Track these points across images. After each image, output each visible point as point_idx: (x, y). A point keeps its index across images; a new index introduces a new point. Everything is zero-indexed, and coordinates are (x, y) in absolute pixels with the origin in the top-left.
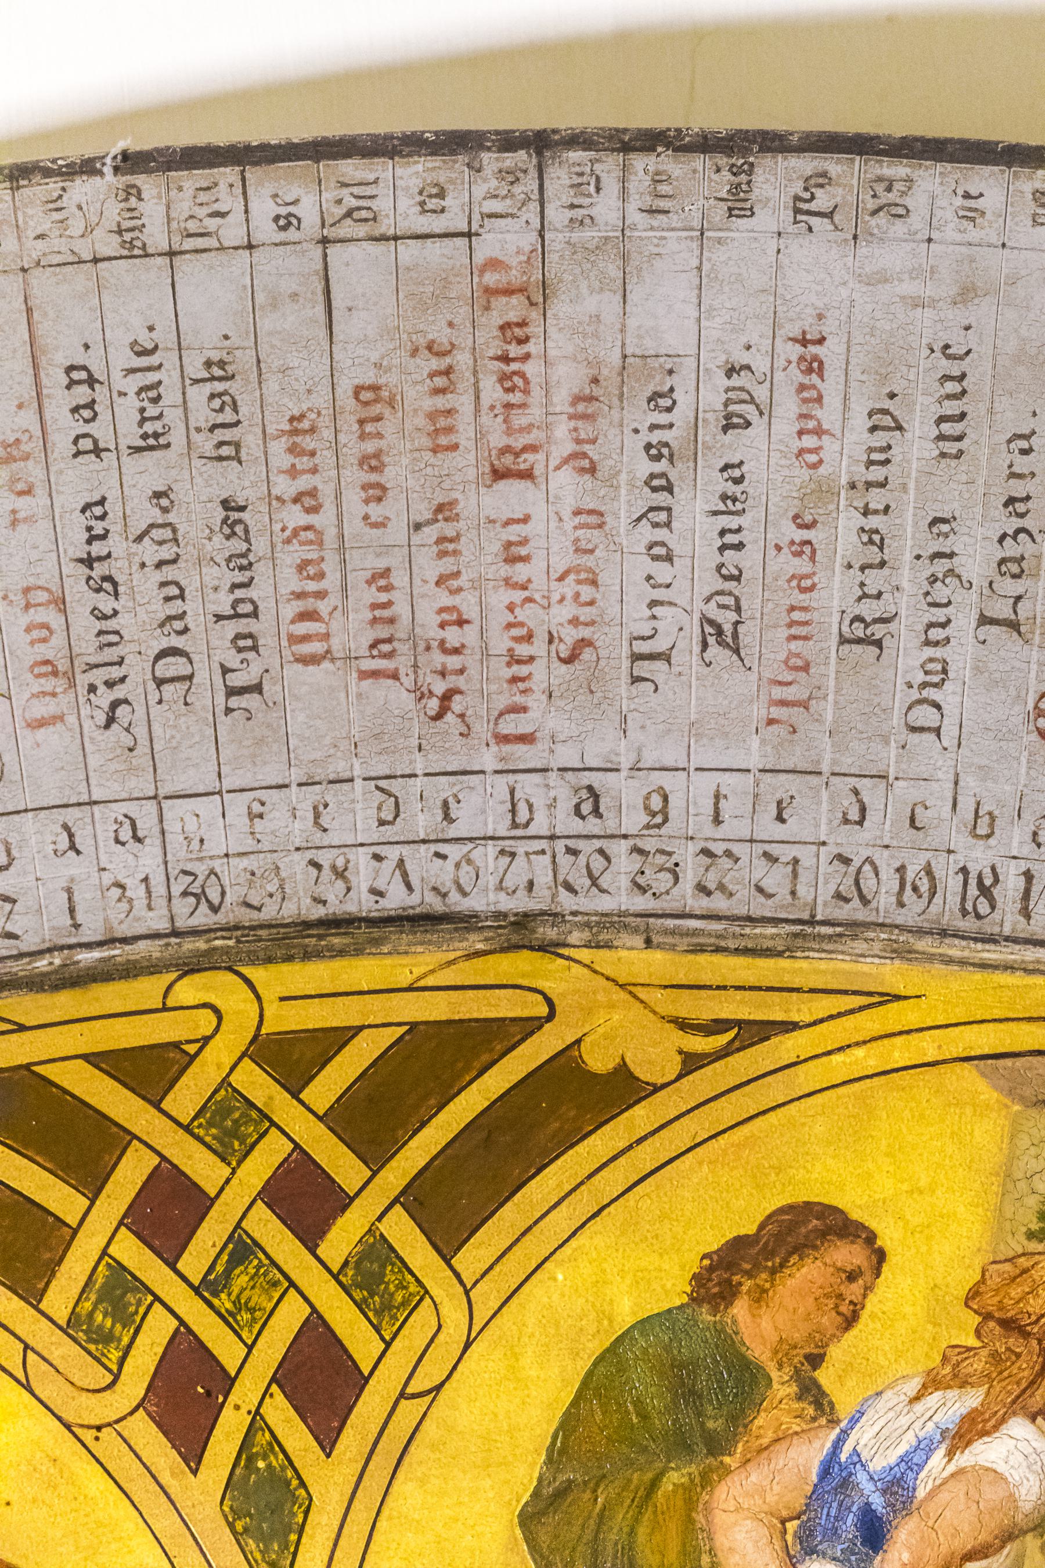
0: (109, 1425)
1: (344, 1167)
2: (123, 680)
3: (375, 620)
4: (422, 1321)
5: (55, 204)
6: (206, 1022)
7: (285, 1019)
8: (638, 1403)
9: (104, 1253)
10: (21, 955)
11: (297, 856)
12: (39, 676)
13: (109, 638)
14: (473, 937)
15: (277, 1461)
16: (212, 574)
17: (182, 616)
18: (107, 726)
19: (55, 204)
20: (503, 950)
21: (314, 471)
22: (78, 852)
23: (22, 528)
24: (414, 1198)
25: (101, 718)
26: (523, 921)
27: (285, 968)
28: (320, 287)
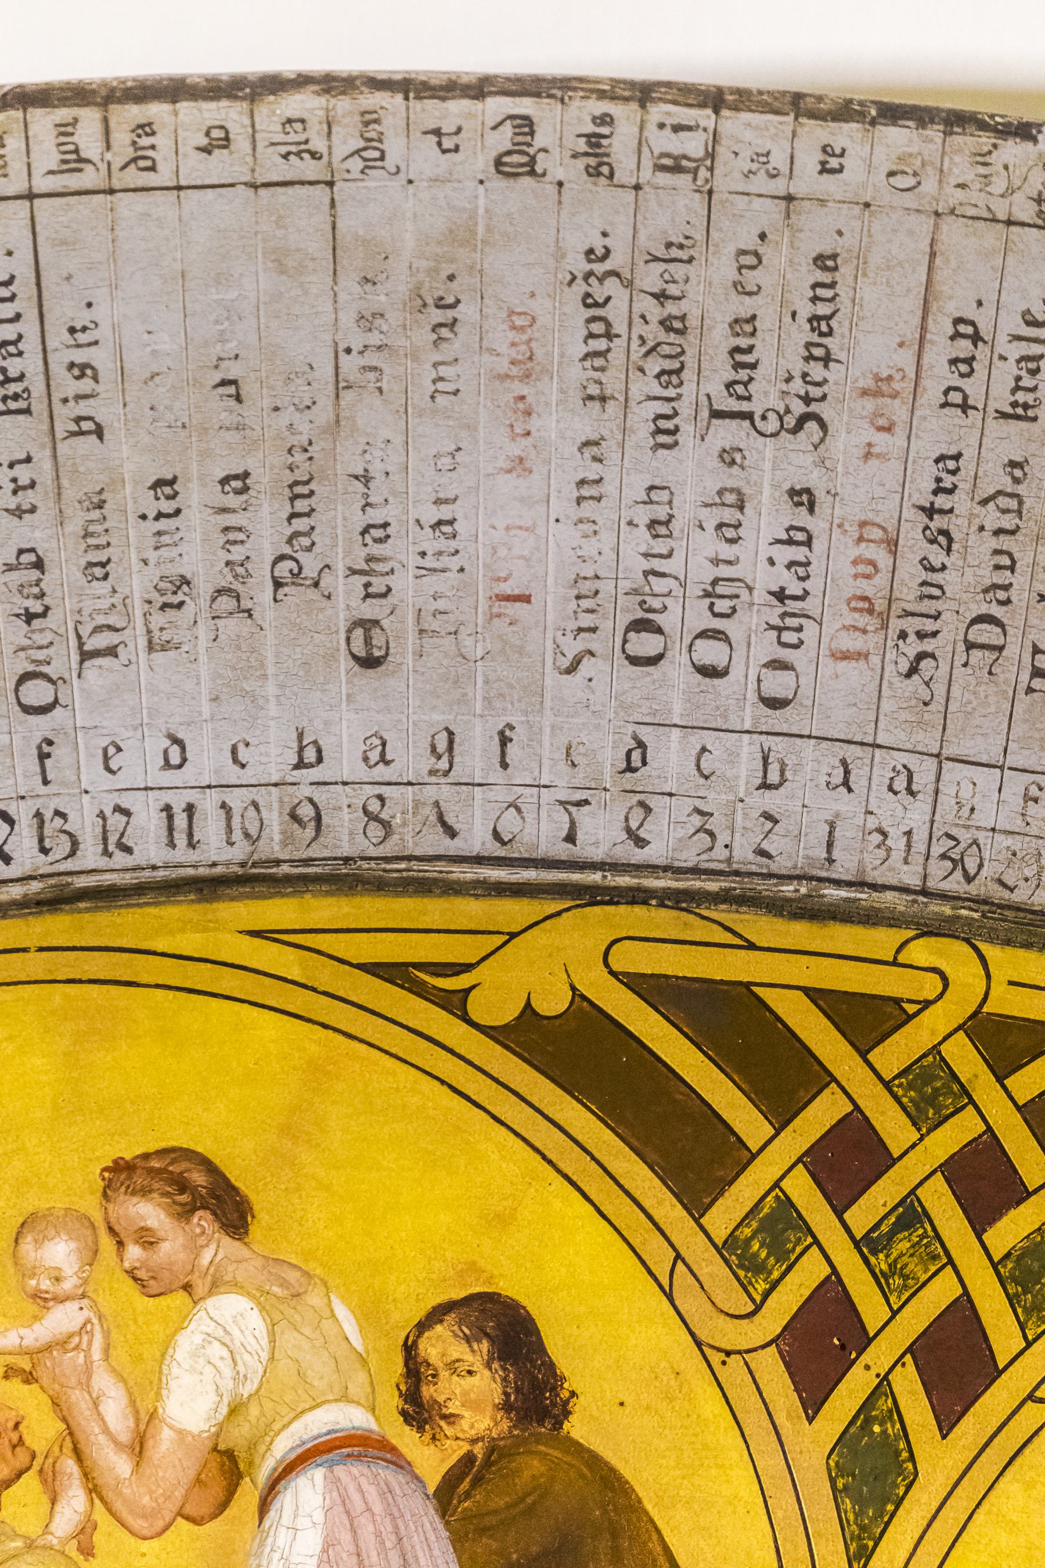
0: (739, 1352)
2: (935, 634)
5: (982, 159)
6: (931, 986)
9: (777, 1185)
10: (771, 875)
12: (855, 610)
15: (893, 1429)
17: (1006, 588)
18: (908, 675)
19: (982, 159)
22: (850, 790)
23: (874, 462)
25: (904, 666)
27: (1021, 953)
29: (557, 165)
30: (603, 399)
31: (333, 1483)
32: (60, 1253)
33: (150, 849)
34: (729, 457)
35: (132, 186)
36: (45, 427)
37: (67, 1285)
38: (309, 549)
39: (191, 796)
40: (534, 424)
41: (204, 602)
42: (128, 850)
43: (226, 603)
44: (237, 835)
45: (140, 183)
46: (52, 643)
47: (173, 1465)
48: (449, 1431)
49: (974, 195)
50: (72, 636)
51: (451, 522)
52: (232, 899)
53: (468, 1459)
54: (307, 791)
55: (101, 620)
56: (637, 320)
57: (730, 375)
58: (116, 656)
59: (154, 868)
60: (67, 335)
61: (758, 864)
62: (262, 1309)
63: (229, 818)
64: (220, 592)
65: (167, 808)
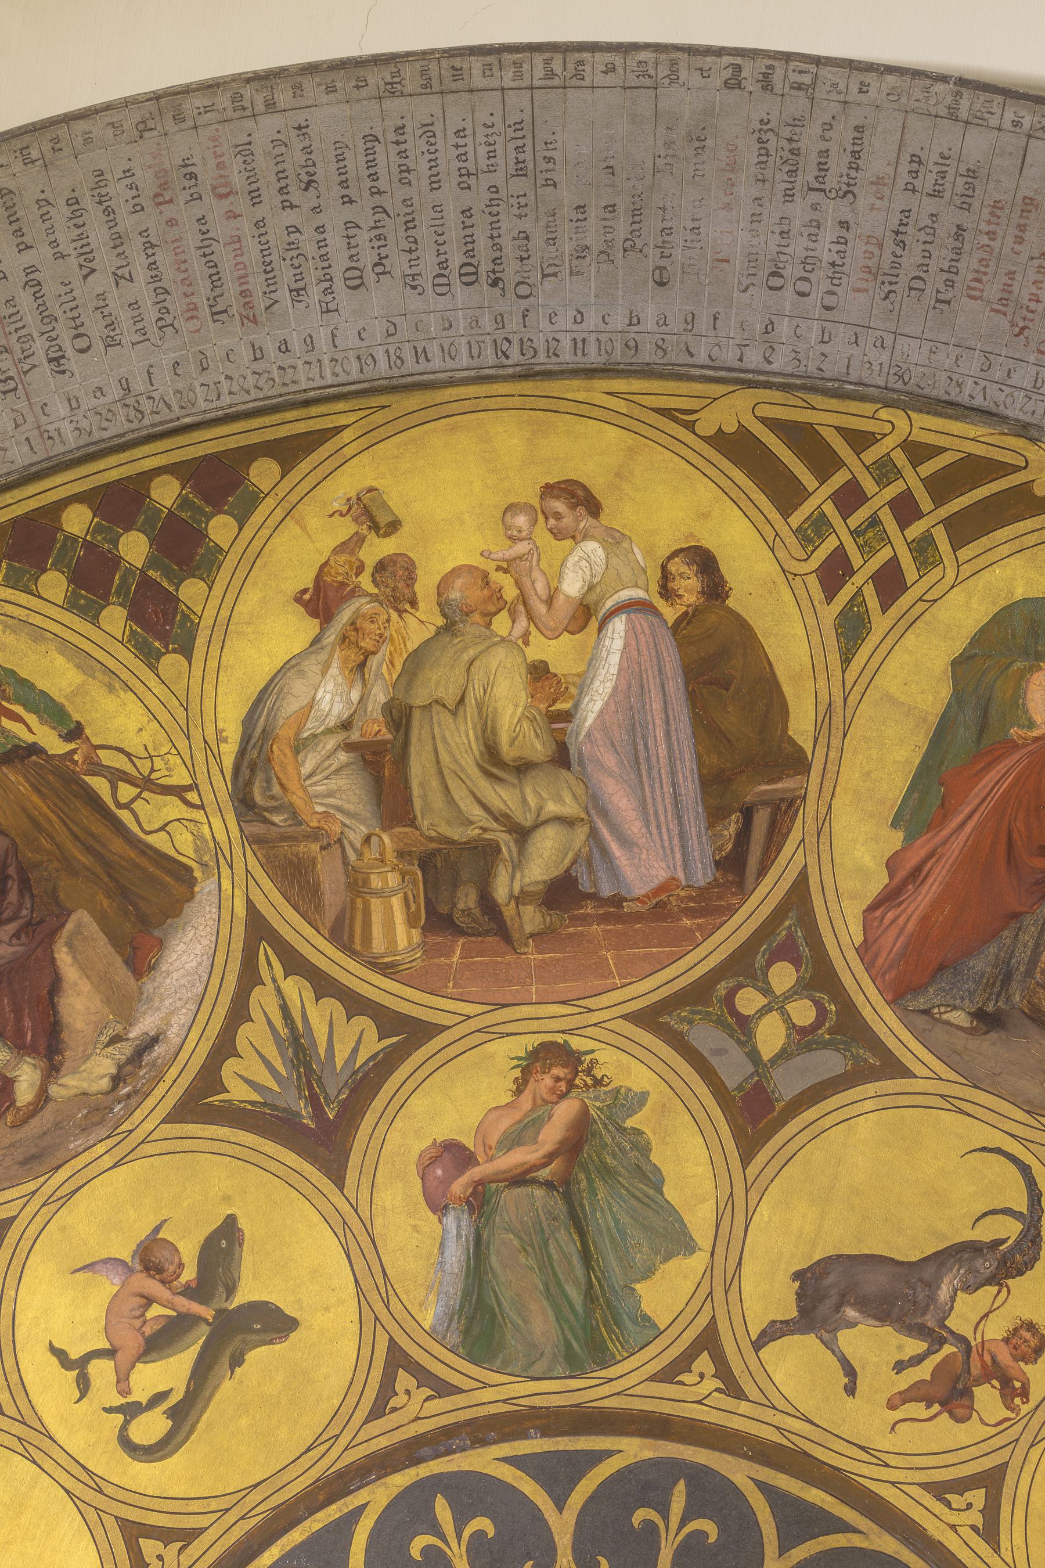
1: (925, 502)
2: (896, 283)
3: (1004, 290)
4: (937, 572)
6: (888, 428)
7: (919, 436)
8: (1013, 631)
9: (819, 507)
10: (823, 379)
11: (944, 373)
13: (896, 265)
14: (1004, 426)
15: (862, 610)
16: (944, 252)
18: (884, 299)
19: (926, 90)
20: (1015, 436)
21: (998, 224)
23: (874, 212)
24: (948, 523)
25: (883, 295)
26: (1026, 426)
27: (925, 416)
28: (1022, 153)
29: (750, 86)
30: (764, 181)
31: (629, 621)
32: (521, 520)
33: (567, 356)
34: (814, 207)
37: (524, 534)
38: (639, 237)
39: (585, 335)
40: (735, 189)
41: (594, 256)
42: (557, 356)
43: (603, 257)
44: (603, 352)
47: (563, 610)
48: (678, 601)
49: (922, 105)
51: (698, 228)
53: (686, 613)
54: (633, 335)
55: (551, 262)
56: (780, 149)
57: (817, 173)
61: (818, 374)
62: (604, 548)
65: (575, 339)
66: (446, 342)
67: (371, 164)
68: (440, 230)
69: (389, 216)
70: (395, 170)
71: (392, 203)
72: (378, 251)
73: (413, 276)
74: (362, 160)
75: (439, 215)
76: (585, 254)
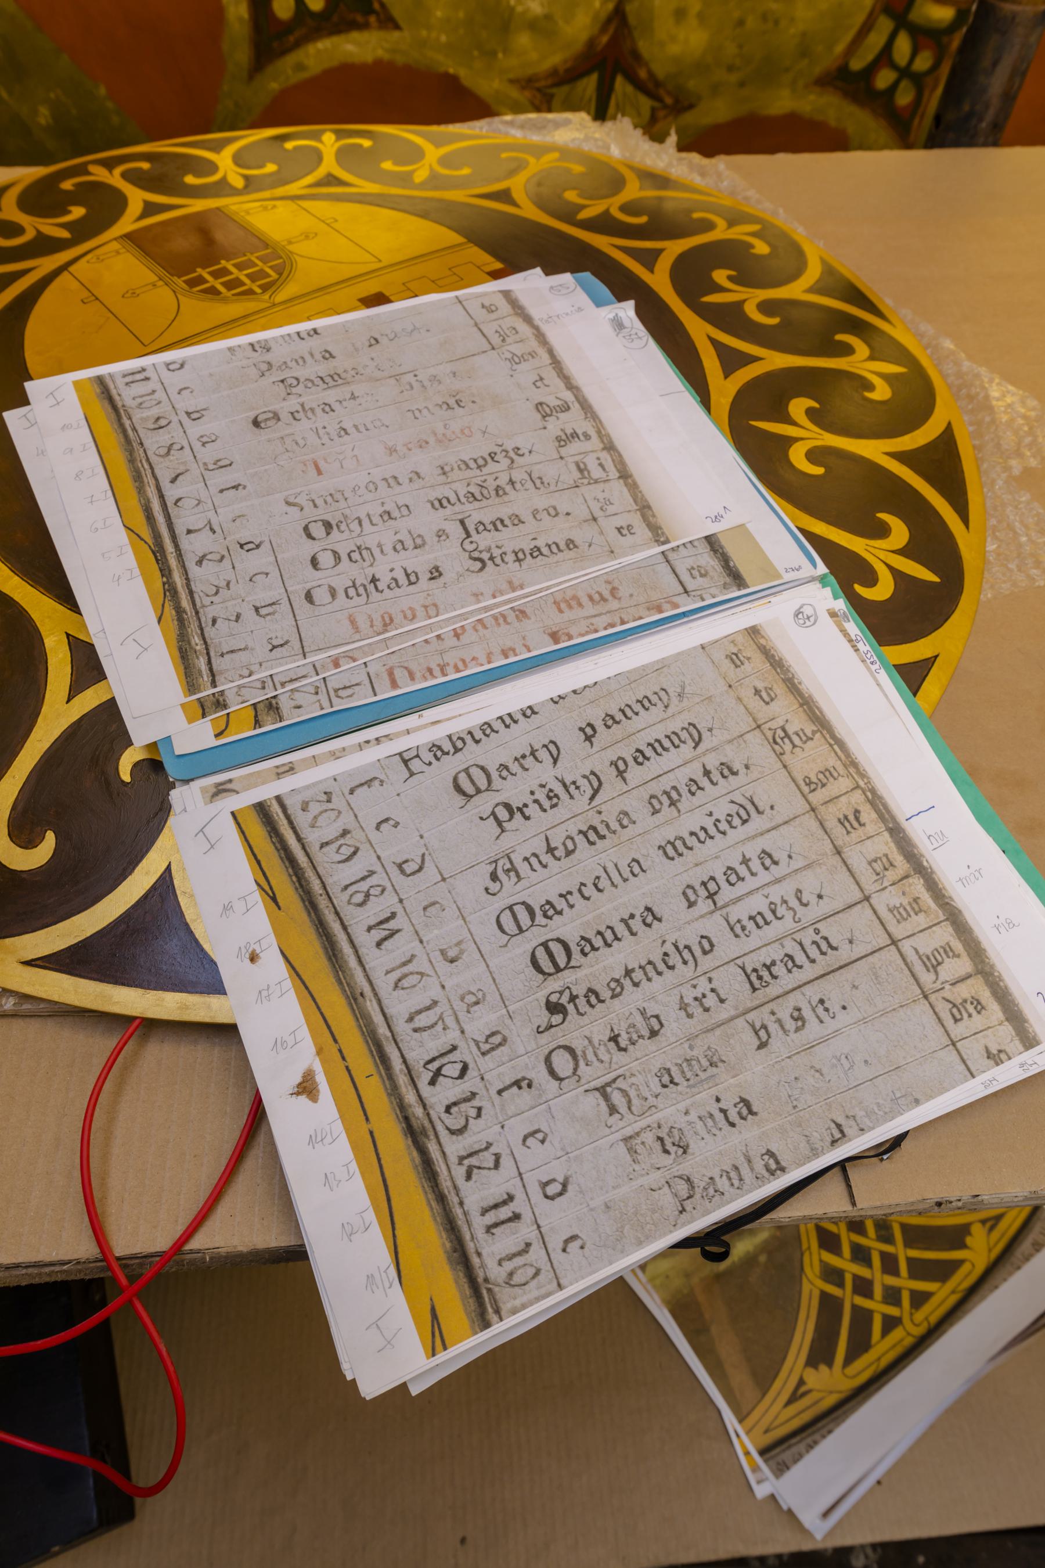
33: (475, 1195)
35: (937, 1010)
36: (749, 1005)
41: (677, 1170)
42: (469, 1177)
43: (682, 1188)
44: (509, 1266)
45: (942, 1015)
46: (602, 1062)
50: (613, 1075)
52: (456, 1282)
55: (632, 1093)
58: (611, 1115)
59: (461, 1204)
60: (817, 1000)
63: (519, 1254)
64: (688, 1180)
65: (511, 1198)
66: (421, 964)
67: (658, 747)
68: (604, 883)
69: (592, 798)
70: (666, 783)
71: (614, 798)
72: (529, 802)
73: (513, 869)
74: (658, 732)
75: (626, 873)
76: (672, 1149)
